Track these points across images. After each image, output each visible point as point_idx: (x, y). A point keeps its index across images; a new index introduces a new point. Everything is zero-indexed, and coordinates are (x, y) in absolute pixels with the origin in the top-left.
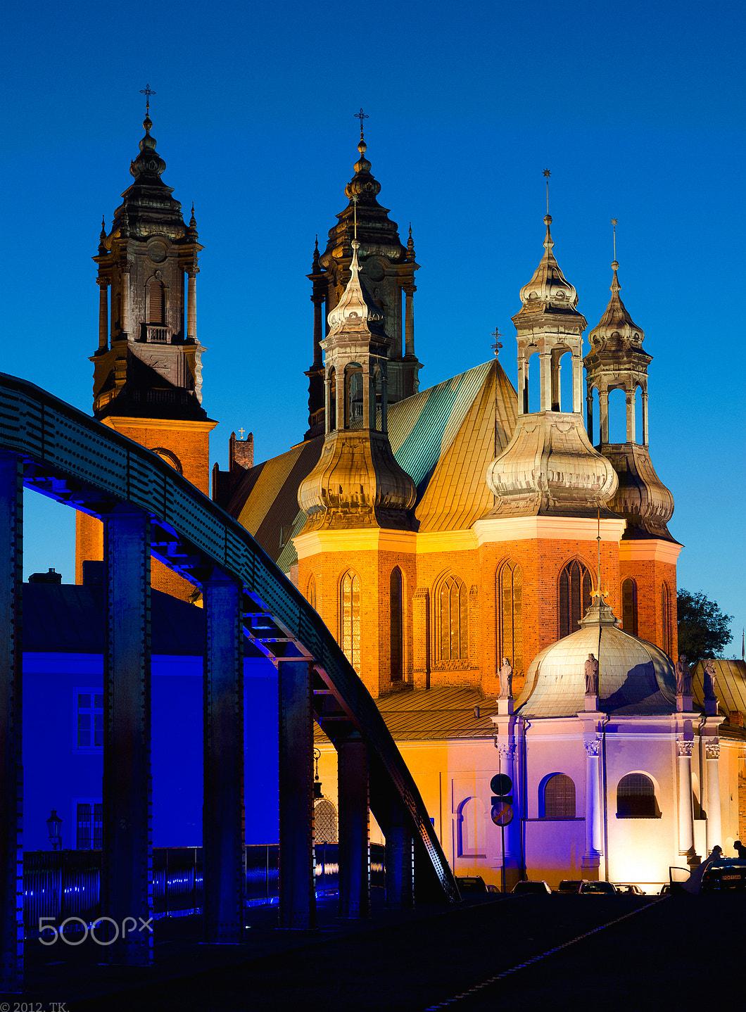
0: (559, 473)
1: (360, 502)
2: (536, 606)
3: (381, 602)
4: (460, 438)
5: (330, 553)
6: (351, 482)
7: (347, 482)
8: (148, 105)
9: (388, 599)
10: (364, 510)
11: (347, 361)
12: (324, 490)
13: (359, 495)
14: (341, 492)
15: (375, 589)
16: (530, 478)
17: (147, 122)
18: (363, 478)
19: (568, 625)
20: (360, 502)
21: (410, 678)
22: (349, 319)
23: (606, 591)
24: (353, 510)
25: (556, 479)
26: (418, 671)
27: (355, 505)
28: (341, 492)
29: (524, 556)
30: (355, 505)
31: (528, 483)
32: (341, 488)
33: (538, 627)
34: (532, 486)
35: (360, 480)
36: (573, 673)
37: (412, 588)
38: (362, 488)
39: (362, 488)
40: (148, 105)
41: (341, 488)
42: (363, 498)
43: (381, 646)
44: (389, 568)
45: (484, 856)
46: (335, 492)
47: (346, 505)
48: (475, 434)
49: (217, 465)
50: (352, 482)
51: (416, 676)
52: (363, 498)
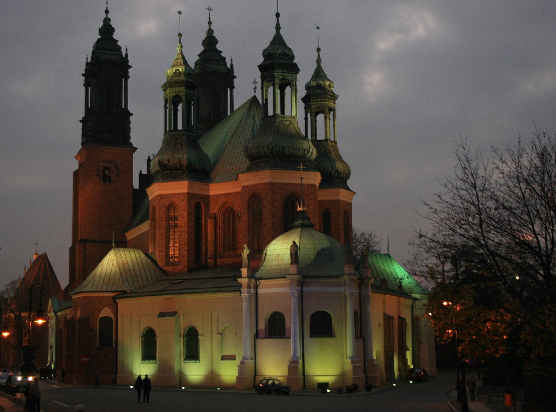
0: (282, 147)
1: (179, 167)
5: (163, 195)
8: (107, 4)
11: (173, 94)
14: (168, 161)
15: (186, 214)
16: (266, 150)
17: (107, 12)
20: (179, 167)
21: (206, 262)
22: (175, 73)
25: (281, 149)
26: (210, 258)
27: (176, 169)
28: (168, 161)
31: (265, 152)
34: (267, 153)
37: (207, 213)
38: (179, 159)
39: (179, 159)
40: (107, 4)
42: (180, 165)
43: (189, 243)
46: (166, 162)
49: (141, 171)
51: (209, 261)
52: (180, 165)
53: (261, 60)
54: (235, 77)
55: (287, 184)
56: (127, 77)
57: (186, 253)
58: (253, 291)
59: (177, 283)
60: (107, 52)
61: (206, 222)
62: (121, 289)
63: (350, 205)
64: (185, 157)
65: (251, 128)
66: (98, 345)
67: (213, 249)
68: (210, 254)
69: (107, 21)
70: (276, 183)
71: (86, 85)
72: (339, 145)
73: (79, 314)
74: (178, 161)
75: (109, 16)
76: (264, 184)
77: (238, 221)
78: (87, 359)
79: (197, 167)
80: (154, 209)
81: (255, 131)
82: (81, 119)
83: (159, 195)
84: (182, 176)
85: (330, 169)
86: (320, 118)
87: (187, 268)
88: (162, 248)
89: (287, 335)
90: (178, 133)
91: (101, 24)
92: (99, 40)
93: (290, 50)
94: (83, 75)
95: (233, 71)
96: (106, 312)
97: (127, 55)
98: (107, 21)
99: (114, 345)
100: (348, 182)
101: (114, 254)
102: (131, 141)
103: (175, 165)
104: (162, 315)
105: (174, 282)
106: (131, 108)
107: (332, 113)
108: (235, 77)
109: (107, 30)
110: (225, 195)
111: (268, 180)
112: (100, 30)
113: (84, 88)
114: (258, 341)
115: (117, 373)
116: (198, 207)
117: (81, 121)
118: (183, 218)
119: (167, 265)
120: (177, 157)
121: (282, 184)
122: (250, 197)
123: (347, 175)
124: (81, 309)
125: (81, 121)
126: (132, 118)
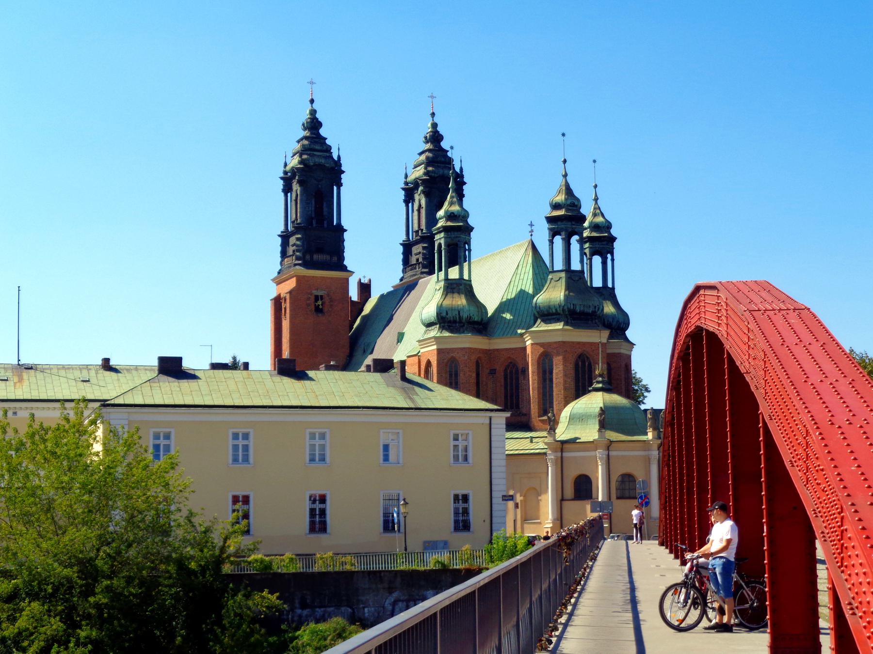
4: (512, 283)
9: (474, 375)
17: (312, 101)
19: (580, 389)
23: (599, 369)
30: (455, 322)
44: (474, 358)
46: (444, 314)
47: (450, 322)
53: (548, 212)
54: (465, 183)
55: (579, 343)
56: (339, 185)
58: (559, 454)
63: (629, 357)
69: (313, 112)
70: (569, 342)
71: (287, 189)
72: (617, 292)
75: (315, 106)
76: (556, 343)
77: (521, 377)
80: (429, 363)
82: (279, 233)
85: (611, 320)
91: (305, 116)
92: (305, 138)
93: (578, 200)
94: (281, 178)
95: (462, 176)
97: (339, 157)
98: (313, 112)
100: (627, 333)
102: (345, 263)
106: (343, 223)
107: (609, 256)
108: (465, 183)
109: (314, 125)
110: (507, 350)
111: (560, 339)
112: (303, 125)
113: (283, 194)
114: (565, 503)
116: (477, 364)
117: (279, 236)
121: (573, 342)
123: (627, 324)
125: (279, 236)
126: (346, 235)
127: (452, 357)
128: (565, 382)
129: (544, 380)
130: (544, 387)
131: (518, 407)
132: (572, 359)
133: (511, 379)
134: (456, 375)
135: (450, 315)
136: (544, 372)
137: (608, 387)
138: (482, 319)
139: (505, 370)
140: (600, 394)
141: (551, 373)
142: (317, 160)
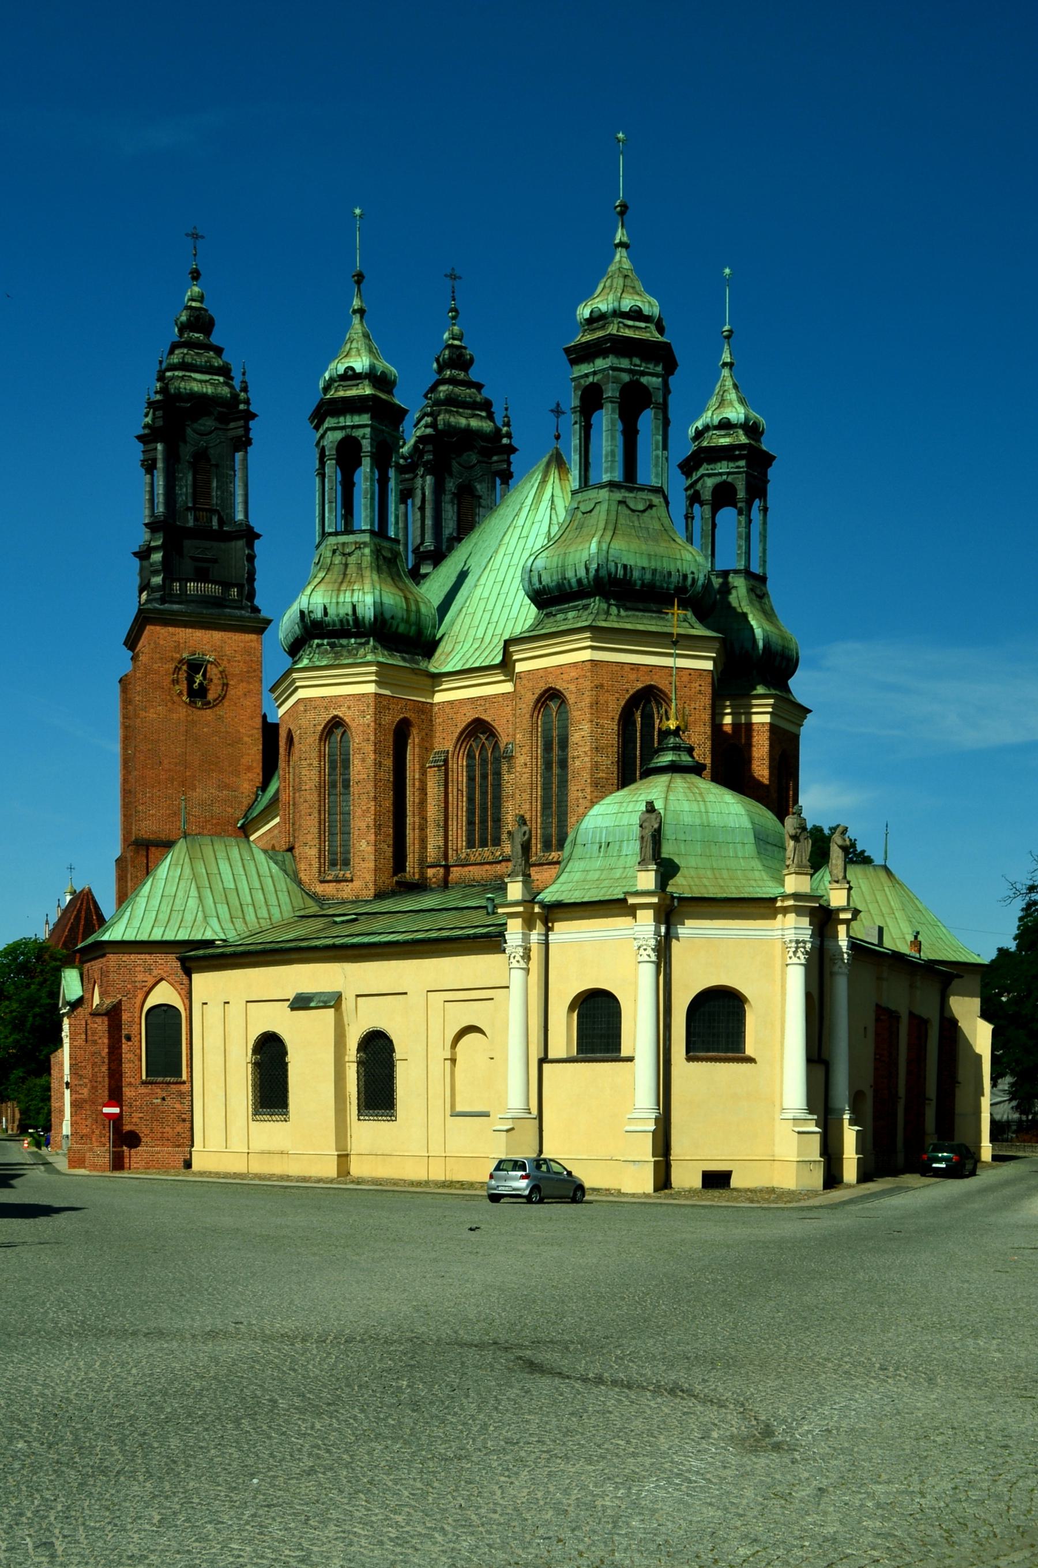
2: (587, 759)
3: (378, 765)
5: (310, 699)
6: (341, 600)
7: (334, 600)
9: (389, 762)
10: (359, 641)
12: (302, 613)
13: (350, 618)
14: (326, 613)
18: (356, 594)
24: (344, 641)
27: (348, 635)
28: (326, 613)
29: (572, 687)
32: (325, 609)
33: (588, 790)
35: (352, 596)
36: (625, 838)
37: (426, 748)
38: (354, 607)
39: (354, 607)
41: (325, 609)
43: (378, 827)
44: (390, 719)
45: (486, 1115)
46: (319, 614)
48: (522, 541)
50: (341, 600)
57: (371, 849)
59: (343, 922)
60: (193, 375)
61: (424, 773)
62: (199, 937)
64: (369, 599)
65: (545, 529)
66: (144, 1077)
67: (441, 843)
68: (432, 853)
73: (96, 1000)
74: (350, 612)
78: (117, 1110)
79: (402, 628)
81: (555, 529)
83: (299, 701)
84: (362, 651)
86: (727, 515)
87: (371, 886)
88: (309, 837)
89: (625, 1052)
90: (350, 538)
96: (164, 994)
99: (184, 1077)
101: (184, 850)
103: (341, 621)
104: (301, 1003)
105: (338, 919)
110: (472, 700)
111: (587, 655)
114: (546, 1067)
115: (192, 1146)
118: (363, 760)
119: (322, 882)
120: (348, 599)
122: (538, 701)
124: (100, 987)
127: (336, 717)
128: (596, 766)
129: (548, 765)
130: (547, 787)
131: (497, 842)
132: (615, 706)
133: (484, 777)
134: (346, 763)
135: (332, 611)
136: (548, 747)
137: (685, 758)
138: (420, 632)
139: (470, 756)
140: (663, 779)
141: (564, 743)
142: (196, 387)
